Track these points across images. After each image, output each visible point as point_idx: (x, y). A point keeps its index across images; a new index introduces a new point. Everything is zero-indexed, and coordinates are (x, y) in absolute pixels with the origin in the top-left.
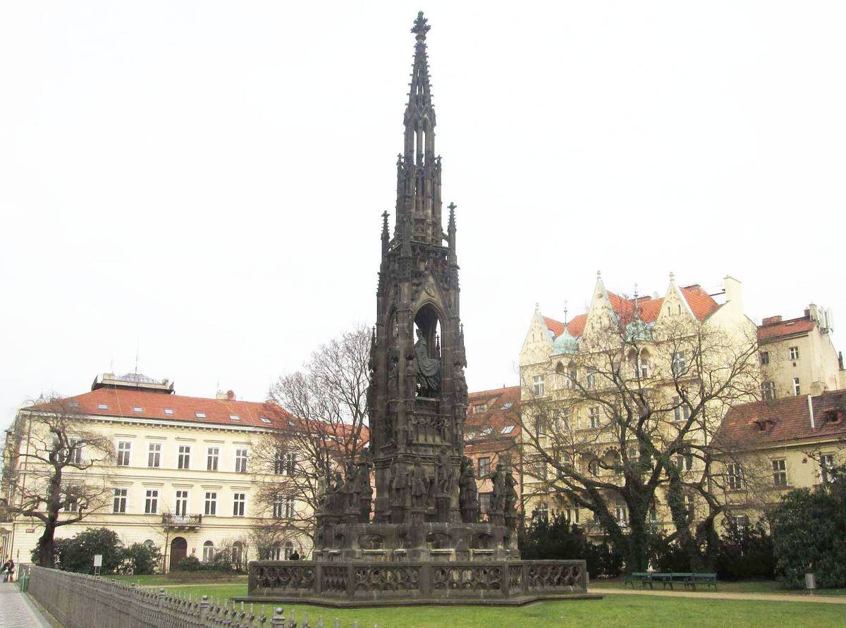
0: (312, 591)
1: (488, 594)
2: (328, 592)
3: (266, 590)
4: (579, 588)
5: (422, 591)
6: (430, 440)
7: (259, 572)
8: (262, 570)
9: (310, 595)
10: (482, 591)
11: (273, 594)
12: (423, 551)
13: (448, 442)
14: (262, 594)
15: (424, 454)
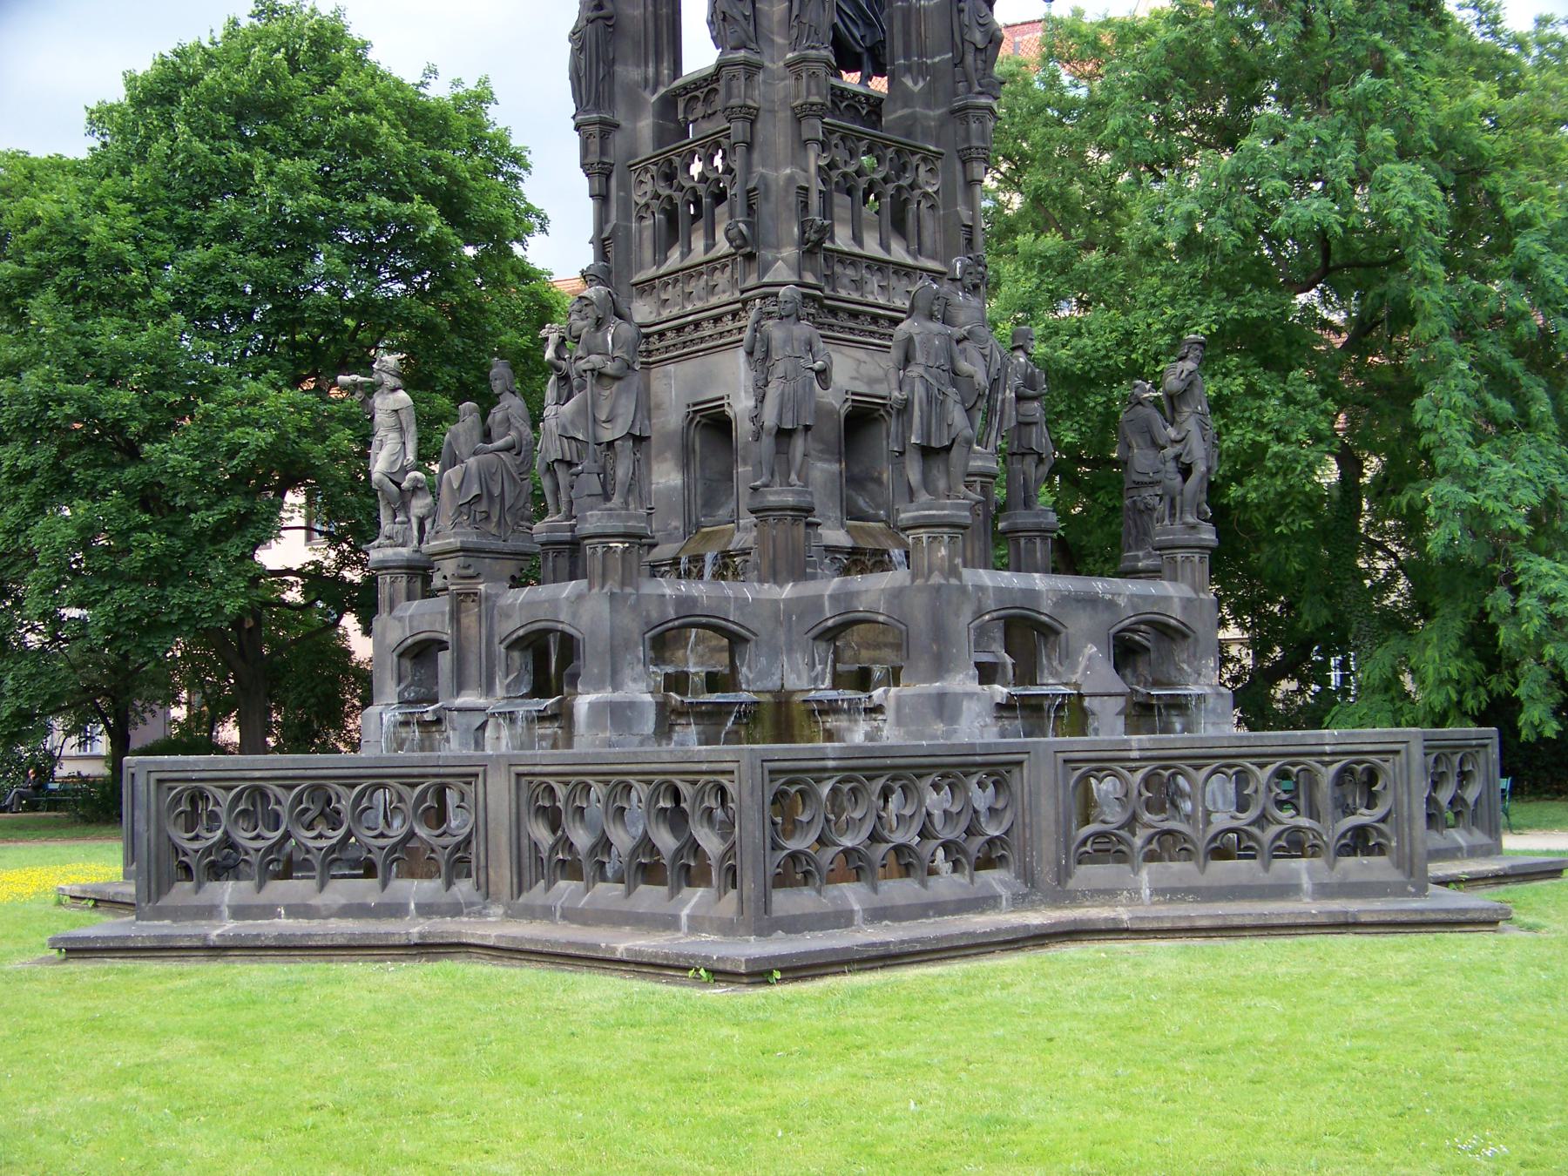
0: (464, 888)
1: (1334, 877)
2: (536, 895)
3: (227, 891)
4: (1479, 838)
5: (1027, 876)
6: (872, 247)
7: (185, 806)
8: (197, 797)
9: (456, 910)
10: (1300, 864)
11: (269, 911)
12: (970, 695)
13: (933, 257)
14: (210, 912)
15: (855, 296)
